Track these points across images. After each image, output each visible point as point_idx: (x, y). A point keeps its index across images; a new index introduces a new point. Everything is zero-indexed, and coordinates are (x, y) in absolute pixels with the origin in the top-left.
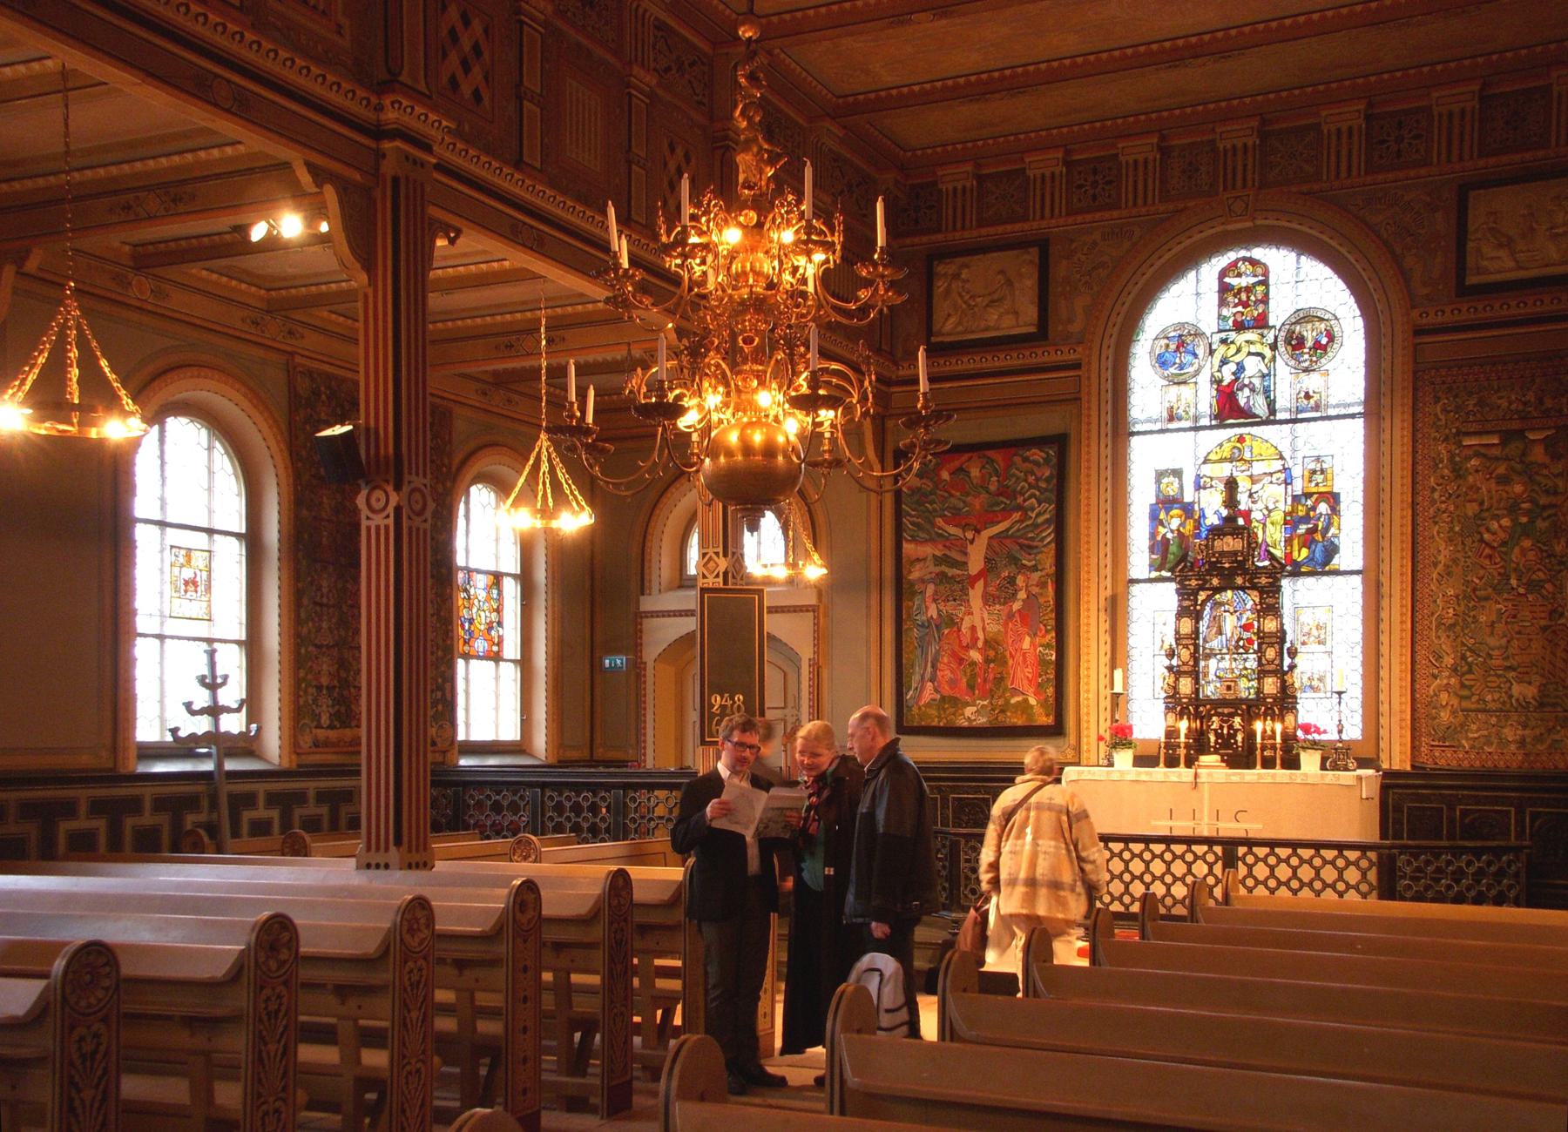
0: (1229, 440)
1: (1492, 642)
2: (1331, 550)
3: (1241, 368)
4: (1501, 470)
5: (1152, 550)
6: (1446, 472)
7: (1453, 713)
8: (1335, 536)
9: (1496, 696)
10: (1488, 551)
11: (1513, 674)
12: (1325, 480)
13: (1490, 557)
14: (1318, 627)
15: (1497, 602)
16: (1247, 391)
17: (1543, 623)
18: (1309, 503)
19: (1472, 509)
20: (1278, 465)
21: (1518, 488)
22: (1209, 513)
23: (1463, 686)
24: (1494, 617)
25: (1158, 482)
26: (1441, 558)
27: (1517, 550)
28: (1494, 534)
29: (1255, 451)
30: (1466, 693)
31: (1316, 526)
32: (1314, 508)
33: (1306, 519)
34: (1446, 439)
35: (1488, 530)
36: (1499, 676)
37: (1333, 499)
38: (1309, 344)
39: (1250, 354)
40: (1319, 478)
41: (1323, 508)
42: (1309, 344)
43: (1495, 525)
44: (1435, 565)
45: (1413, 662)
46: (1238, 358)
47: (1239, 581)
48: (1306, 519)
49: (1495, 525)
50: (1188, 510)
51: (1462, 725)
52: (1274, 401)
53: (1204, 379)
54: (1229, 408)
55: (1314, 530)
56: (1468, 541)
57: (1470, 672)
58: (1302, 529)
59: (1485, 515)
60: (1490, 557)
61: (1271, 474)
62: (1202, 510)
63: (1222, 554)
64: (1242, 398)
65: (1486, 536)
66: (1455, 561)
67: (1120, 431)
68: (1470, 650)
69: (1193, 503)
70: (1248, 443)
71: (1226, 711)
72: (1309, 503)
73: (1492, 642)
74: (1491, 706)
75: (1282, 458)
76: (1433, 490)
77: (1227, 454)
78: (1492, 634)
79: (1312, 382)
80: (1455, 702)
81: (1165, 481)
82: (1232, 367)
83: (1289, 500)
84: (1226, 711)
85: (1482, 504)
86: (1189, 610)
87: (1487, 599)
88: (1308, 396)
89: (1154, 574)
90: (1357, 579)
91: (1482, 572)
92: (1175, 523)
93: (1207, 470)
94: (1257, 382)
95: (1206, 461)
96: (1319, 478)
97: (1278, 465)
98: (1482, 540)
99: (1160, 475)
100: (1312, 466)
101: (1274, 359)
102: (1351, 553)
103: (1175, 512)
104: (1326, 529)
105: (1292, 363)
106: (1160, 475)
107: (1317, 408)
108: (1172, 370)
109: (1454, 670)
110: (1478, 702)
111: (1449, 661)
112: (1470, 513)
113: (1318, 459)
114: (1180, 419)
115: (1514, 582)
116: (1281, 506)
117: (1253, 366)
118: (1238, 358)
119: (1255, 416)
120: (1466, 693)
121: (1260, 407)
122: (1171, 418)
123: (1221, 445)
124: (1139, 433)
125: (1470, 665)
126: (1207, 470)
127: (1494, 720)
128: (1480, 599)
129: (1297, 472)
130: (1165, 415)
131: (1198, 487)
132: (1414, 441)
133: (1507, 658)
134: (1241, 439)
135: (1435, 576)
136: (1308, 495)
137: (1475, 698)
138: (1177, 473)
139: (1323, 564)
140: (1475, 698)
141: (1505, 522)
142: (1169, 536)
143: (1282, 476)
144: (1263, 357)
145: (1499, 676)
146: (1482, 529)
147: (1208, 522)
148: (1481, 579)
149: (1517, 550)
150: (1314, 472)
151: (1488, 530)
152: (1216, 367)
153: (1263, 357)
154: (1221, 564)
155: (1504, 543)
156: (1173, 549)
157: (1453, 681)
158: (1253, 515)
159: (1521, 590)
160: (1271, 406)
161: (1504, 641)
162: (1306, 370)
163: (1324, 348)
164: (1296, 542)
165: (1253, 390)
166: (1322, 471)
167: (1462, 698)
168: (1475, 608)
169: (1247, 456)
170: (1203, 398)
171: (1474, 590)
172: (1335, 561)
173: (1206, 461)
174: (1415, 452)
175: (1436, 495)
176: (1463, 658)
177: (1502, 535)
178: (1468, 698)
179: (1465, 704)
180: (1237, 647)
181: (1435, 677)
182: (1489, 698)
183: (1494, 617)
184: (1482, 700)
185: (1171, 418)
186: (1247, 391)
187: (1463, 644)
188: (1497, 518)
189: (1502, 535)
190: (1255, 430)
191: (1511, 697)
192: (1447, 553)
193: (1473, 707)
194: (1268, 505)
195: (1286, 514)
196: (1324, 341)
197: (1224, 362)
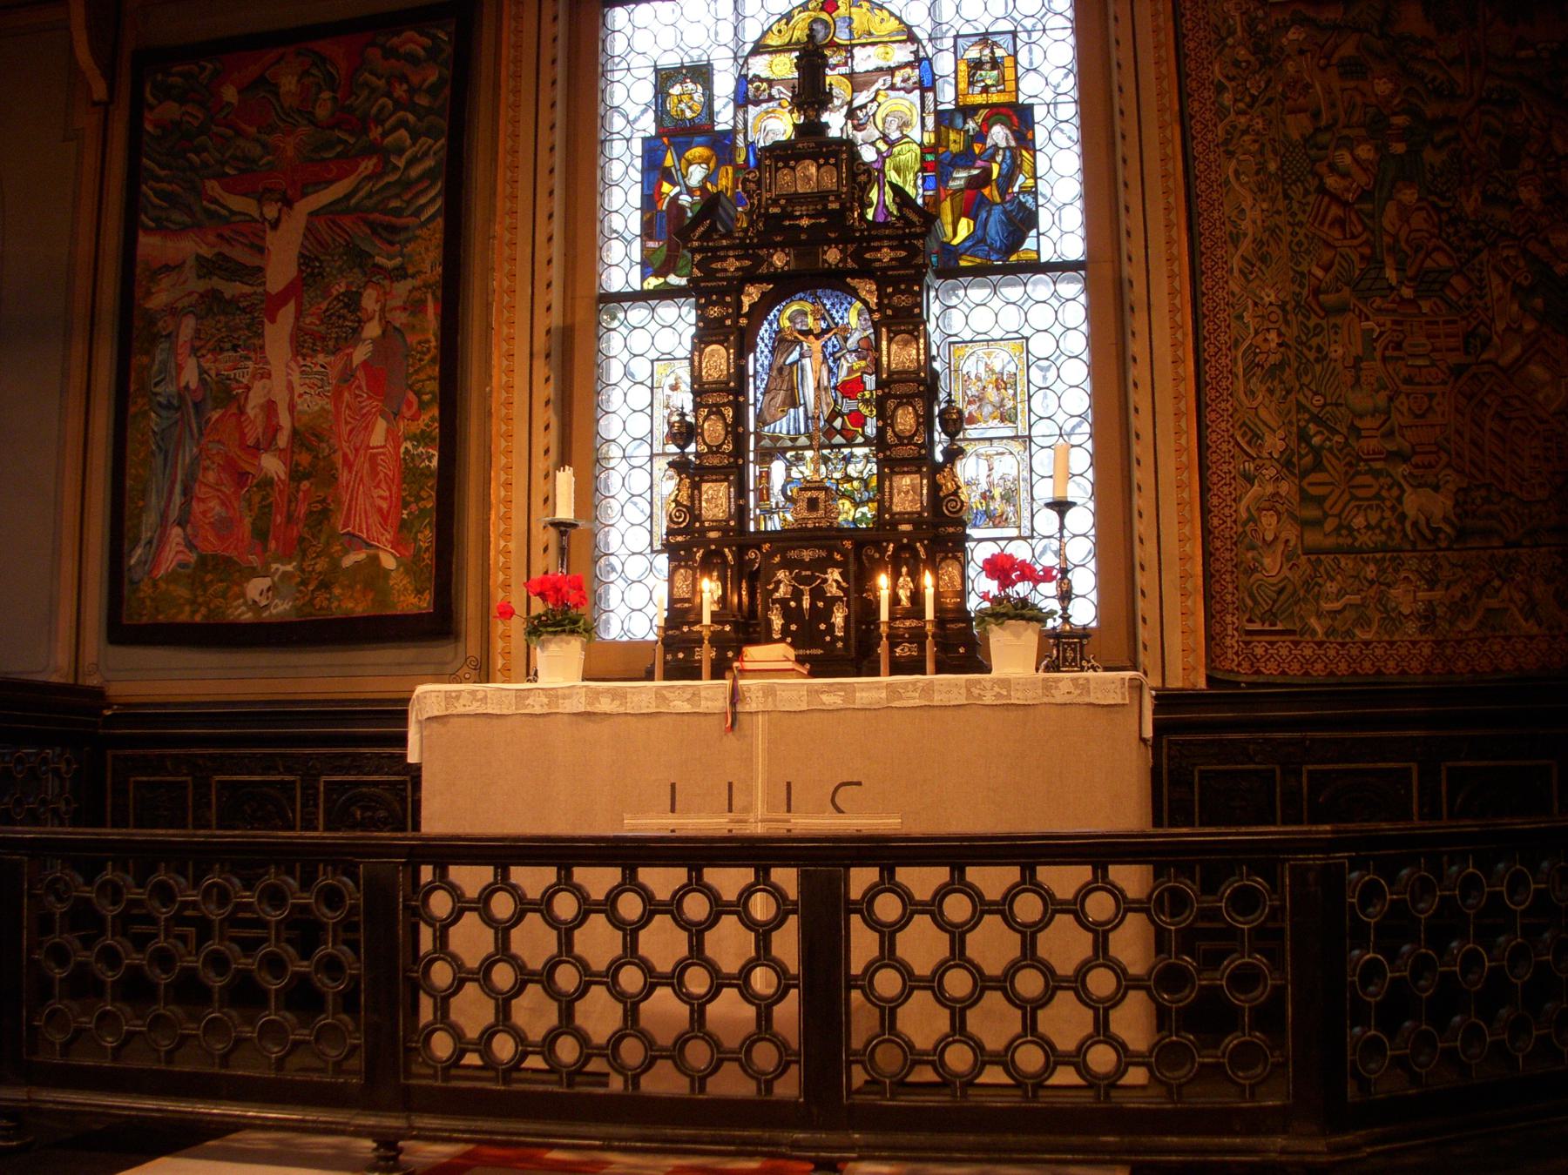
1: (1359, 400)
7: (1288, 557)
8: (1022, 191)
9: (1374, 517)
10: (1335, 211)
11: (1403, 469)
14: (1000, 383)
19: (1297, 127)
20: (902, 54)
23: (1305, 497)
24: (1357, 349)
27: (1391, 210)
28: (1345, 175)
30: (1311, 513)
33: (965, 158)
35: (1332, 168)
36: (1377, 474)
37: (1020, 117)
41: (999, 135)
48: (965, 158)
51: (1308, 584)
56: (1297, 192)
57: (1318, 466)
58: (960, 177)
59: (1324, 138)
60: (1340, 223)
61: (891, 71)
65: (1331, 182)
66: (1274, 231)
68: (1315, 419)
72: (971, 125)
73: (1359, 400)
74: (1365, 539)
76: (1220, 88)
80: (1291, 533)
83: (930, 121)
85: (1316, 116)
87: (1342, 310)
91: (1327, 255)
96: (990, 76)
97: (902, 54)
98: (1322, 190)
100: (974, 53)
111: (1274, 443)
112: (1296, 136)
113: (985, 39)
115: (1391, 274)
116: (915, 133)
120: (1311, 513)
125: (1316, 452)
127: (1370, 571)
128: (1328, 312)
129: (944, 64)
133: (1390, 434)
136: (968, 111)
137: (1330, 525)
139: (1005, 254)
140: (1330, 525)
141: (1365, 152)
145: (1377, 474)
146: (1322, 168)
148: (1326, 269)
149: (1391, 210)
150: (977, 65)
151: (1332, 168)
155: (1365, 195)
157: (1284, 488)
159: (1407, 292)
161: (1381, 399)
166: (995, 63)
167: (1305, 524)
168: (1318, 330)
171: (1316, 292)
172: (1030, 243)
176: (1303, 437)
177: (1362, 179)
178: (1317, 523)
179: (1313, 538)
182: (1359, 522)
184: (1344, 528)
187: (1301, 407)
188: (1348, 143)
189: (1362, 179)
192: (1256, 214)
193: (1330, 542)
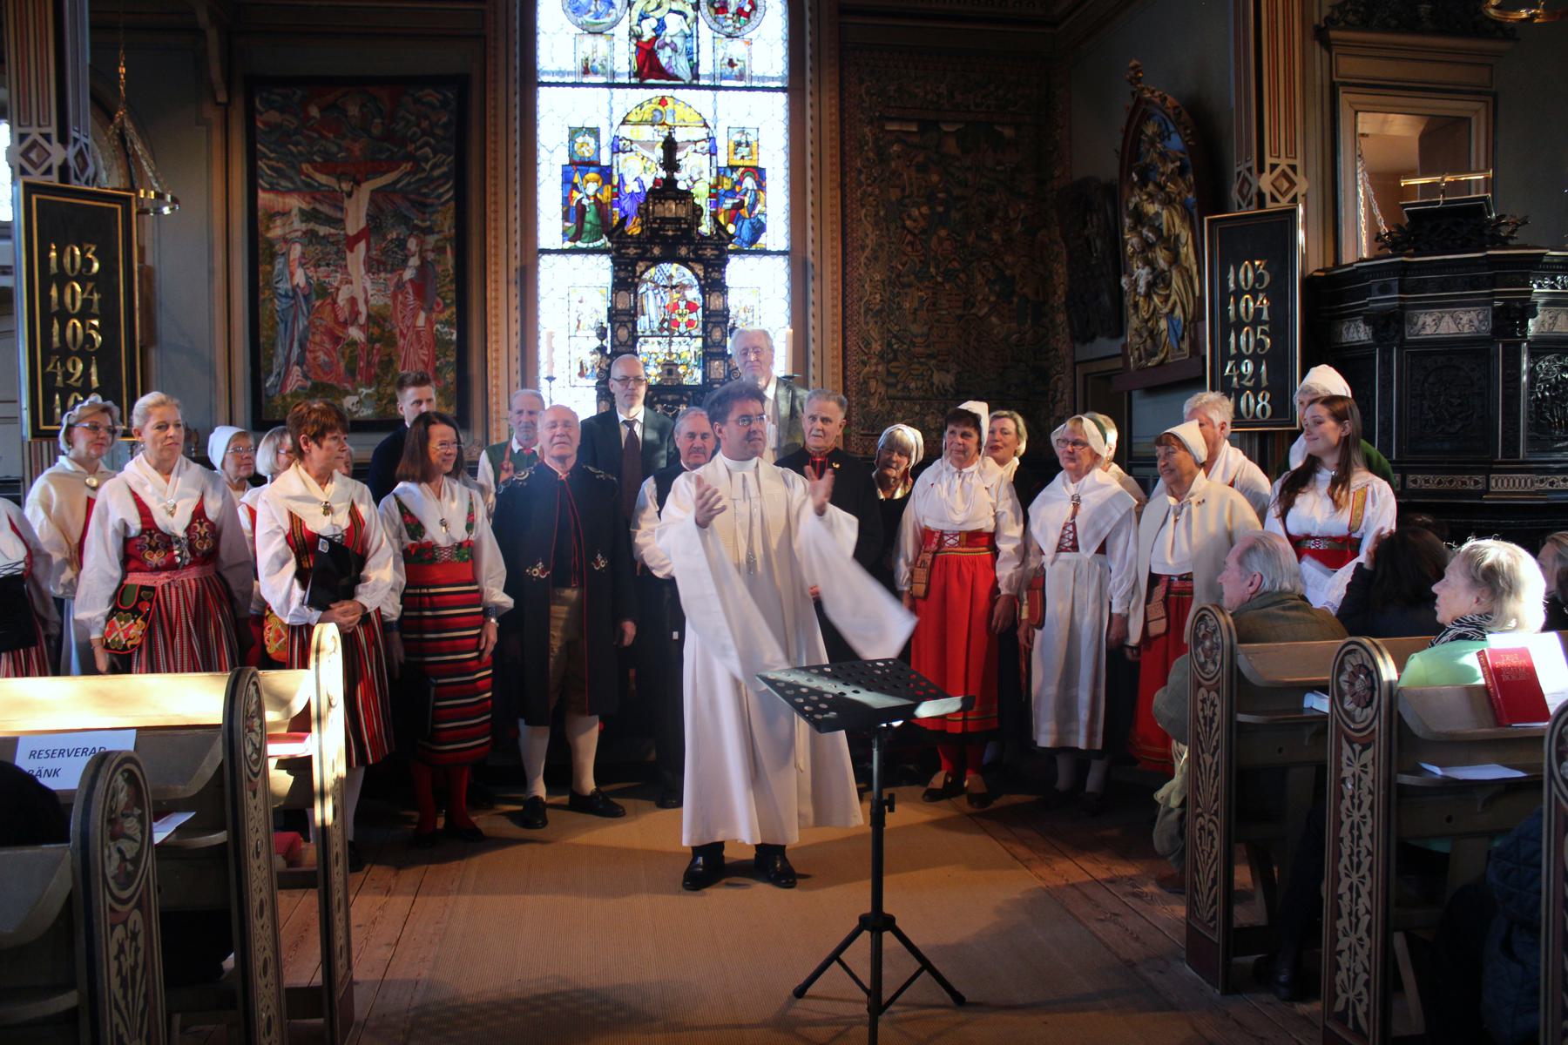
0: (650, 101)
1: (914, 328)
2: (759, 229)
3: (662, 25)
4: (920, 158)
5: (566, 217)
6: (871, 155)
7: (881, 400)
8: (760, 213)
9: (920, 384)
10: (909, 237)
11: (933, 362)
12: (751, 153)
13: (911, 243)
15: (919, 290)
16: (668, 51)
17: (959, 312)
18: (735, 176)
19: (894, 195)
20: (702, 133)
21: (935, 178)
22: (629, 179)
23: (889, 373)
24: (916, 304)
25: (572, 140)
26: (868, 241)
27: (935, 240)
30: (892, 380)
31: (742, 202)
32: (740, 182)
33: (732, 193)
34: (871, 122)
36: (921, 364)
37: (758, 174)
38: (732, 9)
39: (671, 11)
40: (744, 151)
41: (749, 183)
42: (732, 9)
43: (915, 212)
44: (863, 248)
45: (844, 348)
46: (658, 14)
47: (683, 251)
48: (732, 193)
49: (915, 212)
50: (606, 174)
52: (698, 64)
53: (622, 31)
54: (649, 68)
55: (741, 205)
57: (895, 359)
58: (728, 203)
60: (911, 243)
62: (621, 177)
63: (664, 220)
64: (664, 57)
65: (908, 223)
66: (881, 245)
67: (529, 80)
68: (895, 336)
69: (610, 167)
70: (670, 106)
71: (670, 398)
72: (735, 176)
73: (914, 328)
74: (915, 394)
75: (706, 126)
76: (860, 172)
77: (648, 116)
78: (914, 321)
79: (736, 49)
80: (882, 390)
81: (580, 140)
82: (654, 24)
84: (670, 398)
85: (903, 190)
86: (625, 281)
87: (910, 285)
88: (731, 63)
89: (568, 245)
90: (781, 264)
92: (591, 188)
93: (626, 131)
94: (679, 42)
97: (702, 133)
98: (904, 227)
99: (574, 133)
100: (737, 138)
101: (697, 19)
102: (777, 234)
103: (591, 175)
104: (753, 206)
105: (716, 26)
106: (574, 133)
107: (741, 77)
108: (588, 18)
109: (881, 356)
110: (903, 390)
111: (876, 347)
113: (742, 131)
114: (596, 73)
116: (706, 176)
117: (674, 25)
118: (658, 14)
119: (677, 78)
120: (892, 380)
121: (682, 67)
122: (586, 71)
123: (641, 106)
124: (549, 84)
125: (895, 352)
126: (626, 131)
127: (917, 408)
128: (903, 286)
129: (722, 143)
130: (580, 68)
131: (616, 149)
132: (842, 120)
134: (663, 102)
135: (863, 260)
136: (734, 168)
137: (900, 386)
138: (595, 132)
139: (752, 247)
140: (900, 386)
141: (924, 210)
142: (585, 202)
143: (707, 145)
144: (686, 17)
146: (905, 216)
147: (628, 190)
149: (935, 240)
150: (739, 144)
151: (909, 216)
152: (635, 21)
153: (686, 17)
154: (659, 232)
155: (924, 231)
156: (589, 217)
157: (880, 368)
160: (694, 68)
161: (925, 329)
162: (729, 36)
163: (748, 15)
165: (675, 50)
166: (748, 145)
167: (888, 385)
170: (623, 59)
171: (898, 276)
173: (623, 123)
174: (842, 133)
175: (863, 177)
176: (889, 345)
177: (922, 223)
178: (895, 385)
179: (892, 392)
180: (661, 329)
181: (864, 364)
182: (913, 385)
183: (916, 304)
184: (906, 388)
185: (586, 71)
186: (668, 51)
188: (918, 206)
189: (922, 223)
190: (678, 93)
191: (932, 384)
194: (695, 173)
195: (711, 187)
196: (747, 8)
197: (643, 17)
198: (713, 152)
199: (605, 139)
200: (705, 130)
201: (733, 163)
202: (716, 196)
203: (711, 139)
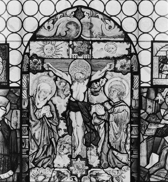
20: (122, 49)
22: (40, 102)
29: (96, 30)
61: (115, 59)
72: (160, 97)
75: (127, 40)
83: (136, 93)
93: (35, 48)
95: (35, 37)
97: (122, 49)
116: (128, 100)
126: (35, 48)
129: (145, 58)
158: (94, 109)
164: (143, 146)
169: (86, 35)
173: (35, 37)
198: (135, 72)
199: (15, 58)
200: (127, 45)
201: (157, 82)
202: (136, 119)
203: (131, 55)
